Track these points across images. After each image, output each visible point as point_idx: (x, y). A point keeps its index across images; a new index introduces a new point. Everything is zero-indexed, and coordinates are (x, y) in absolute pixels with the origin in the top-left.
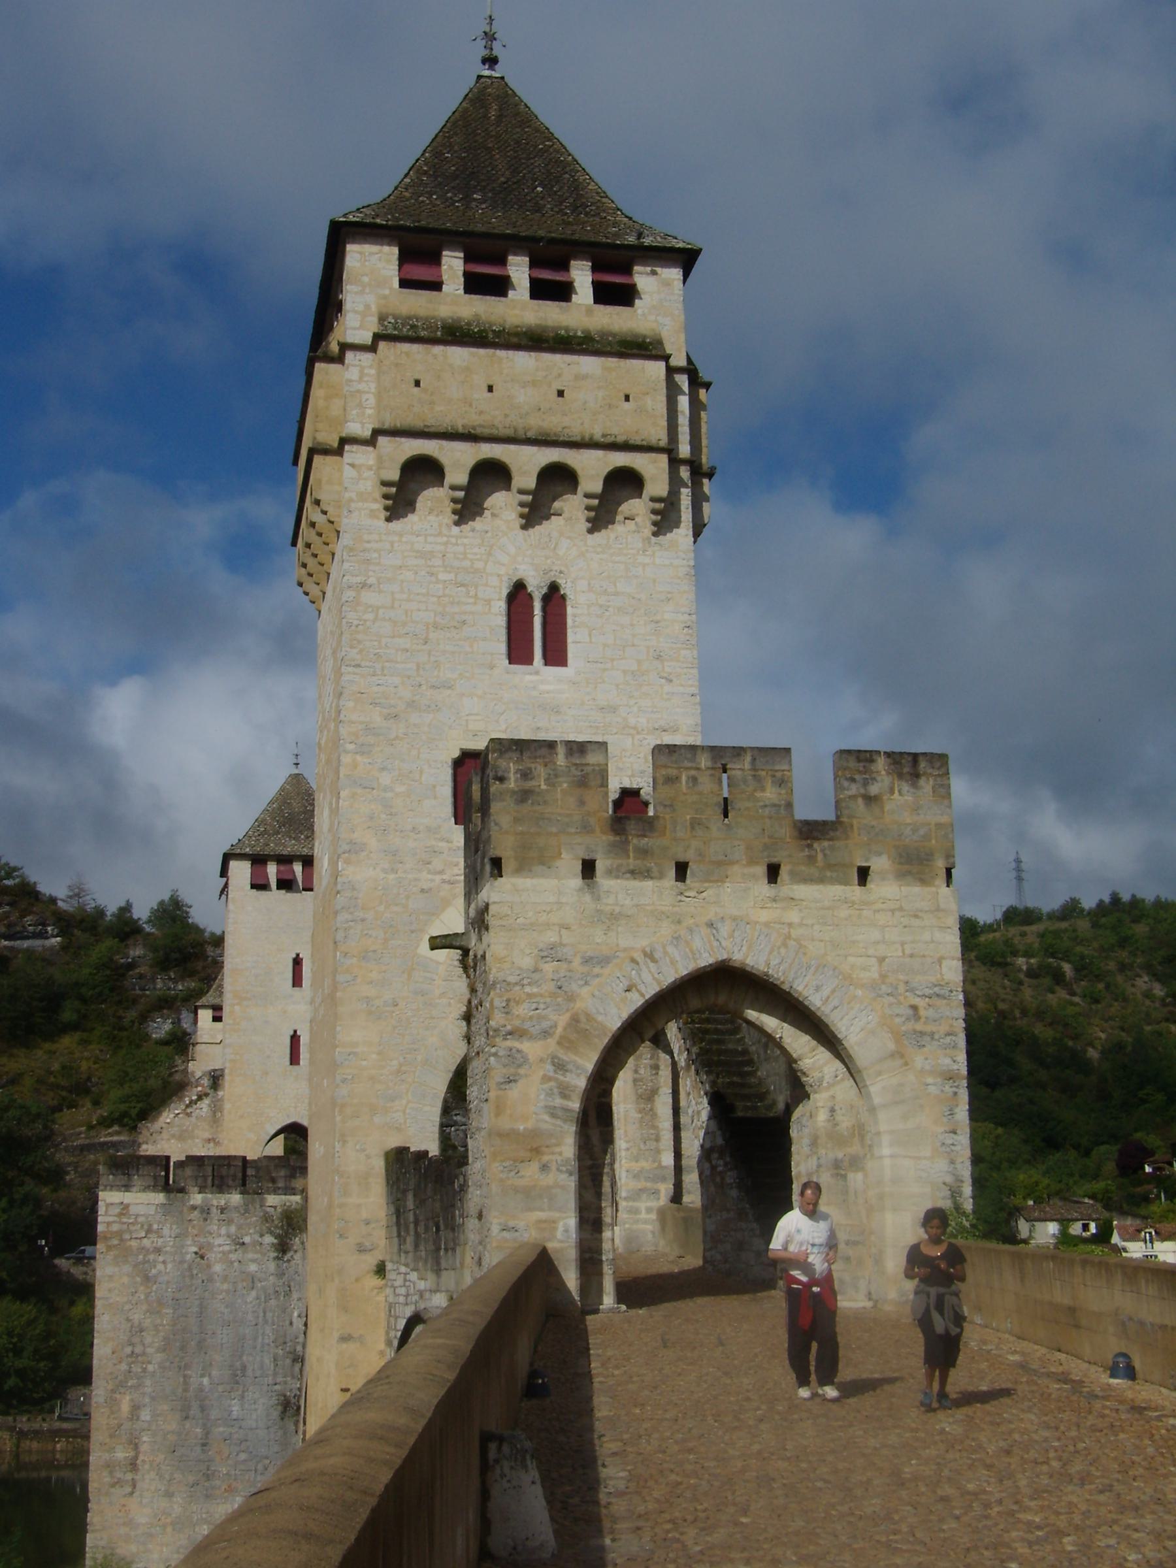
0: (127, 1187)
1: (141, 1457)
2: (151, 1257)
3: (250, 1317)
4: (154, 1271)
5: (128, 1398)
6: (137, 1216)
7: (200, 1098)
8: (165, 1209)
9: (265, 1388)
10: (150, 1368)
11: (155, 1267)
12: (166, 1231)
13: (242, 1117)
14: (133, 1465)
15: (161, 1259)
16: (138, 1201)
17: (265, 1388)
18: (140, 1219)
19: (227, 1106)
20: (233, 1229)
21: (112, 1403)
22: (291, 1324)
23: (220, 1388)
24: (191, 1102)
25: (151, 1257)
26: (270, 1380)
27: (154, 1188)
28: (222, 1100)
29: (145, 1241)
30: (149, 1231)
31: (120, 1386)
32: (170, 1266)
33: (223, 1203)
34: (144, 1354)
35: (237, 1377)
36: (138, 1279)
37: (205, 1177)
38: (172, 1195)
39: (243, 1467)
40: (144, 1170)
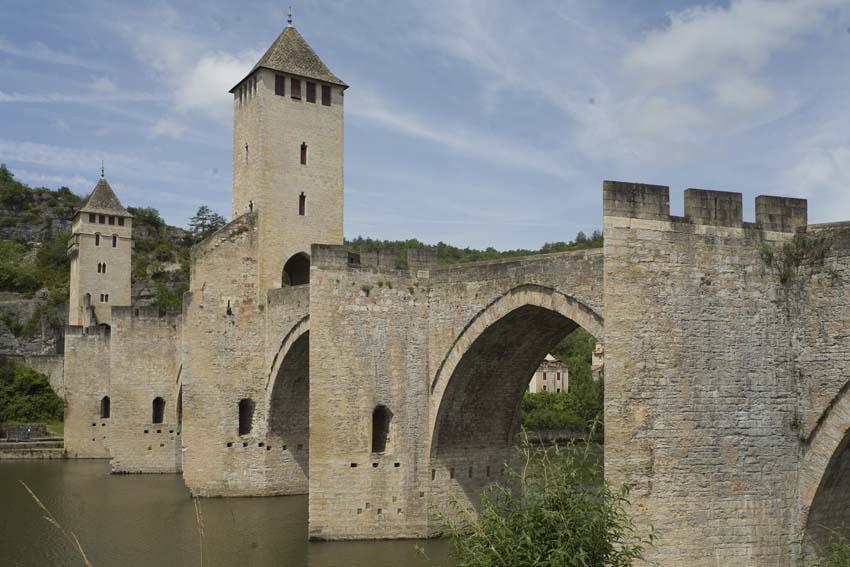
0: (633, 214)
1: (656, 462)
2: (660, 280)
3: (755, 338)
4: (663, 294)
5: (641, 409)
6: (644, 241)
7: (240, 231)
8: (673, 236)
9: (769, 401)
10: (663, 382)
11: (663, 289)
12: (673, 257)
13: (270, 245)
14: (649, 469)
15: (669, 282)
16: (645, 227)
17: (769, 401)
18: (647, 245)
19: (261, 237)
20: (736, 259)
21: (626, 415)
22: (791, 345)
23: (728, 400)
24: (234, 233)
25: (660, 280)
26: (773, 394)
27: (654, 216)
29: (654, 264)
30: (657, 255)
31: (634, 399)
32: (678, 289)
33: (726, 234)
34: (656, 369)
35: (743, 393)
36: (647, 300)
37: (709, 213)
38: (678, 224)
39: (749, 469)
40: (649, 199)
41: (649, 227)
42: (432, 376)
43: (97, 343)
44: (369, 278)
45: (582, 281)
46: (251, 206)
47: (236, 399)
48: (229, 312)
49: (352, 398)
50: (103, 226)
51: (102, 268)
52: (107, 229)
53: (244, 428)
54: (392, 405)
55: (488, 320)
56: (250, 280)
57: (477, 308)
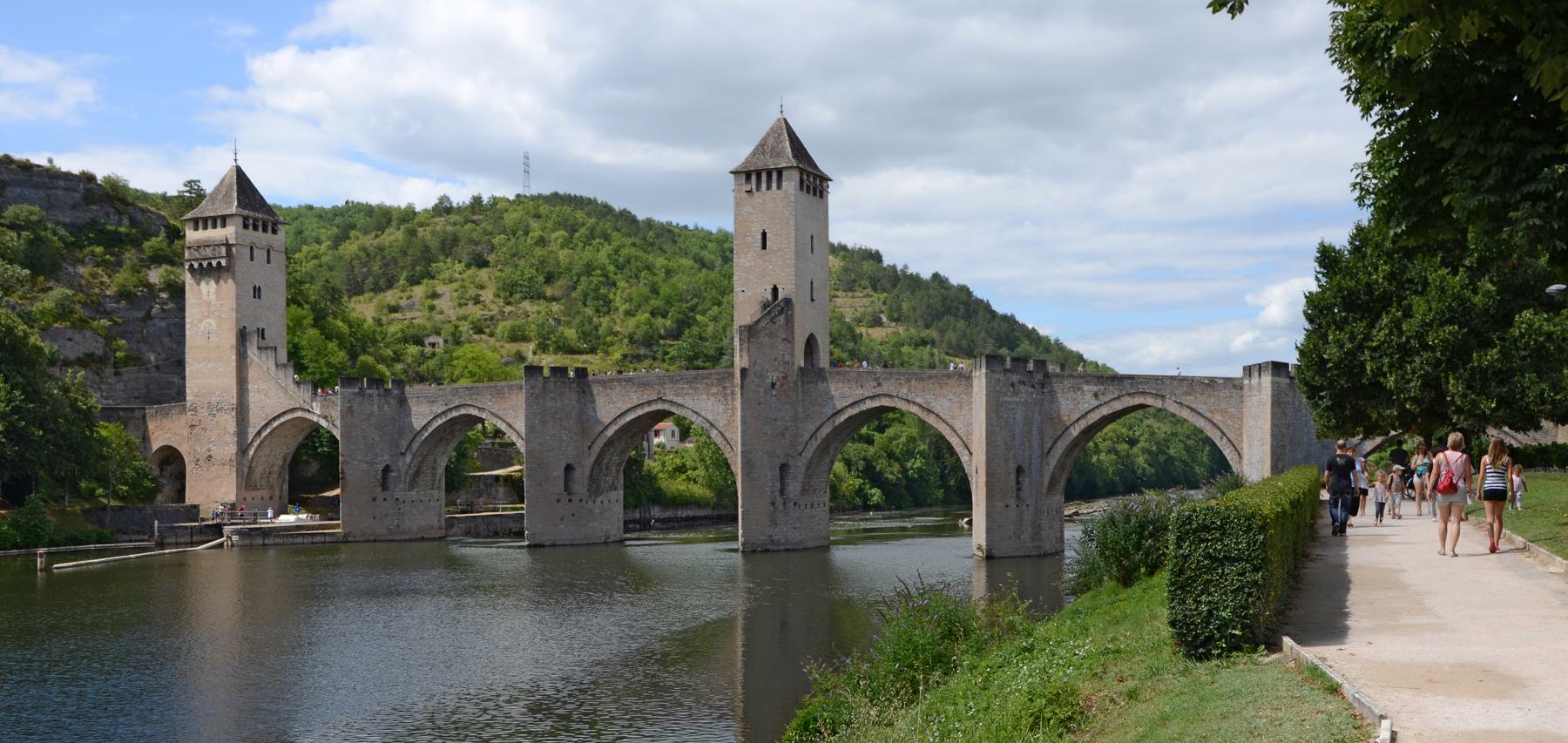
28: (792, 316)
41: (1284, 381)
42: (1048, 446)
43: (376, 400)
44: (1015, 378)
45: (1187, 393)
46: (775, 290)
47: (778, 463)
48: (773, 385)
49: (1007, 461)
50: (256, 234)
51: (257, 292)
52: (260, 237)
53: (782, 492)
54: (1025, 466)
55: (1105, 411)
56: (787, 358)
57: (1096, 403)
